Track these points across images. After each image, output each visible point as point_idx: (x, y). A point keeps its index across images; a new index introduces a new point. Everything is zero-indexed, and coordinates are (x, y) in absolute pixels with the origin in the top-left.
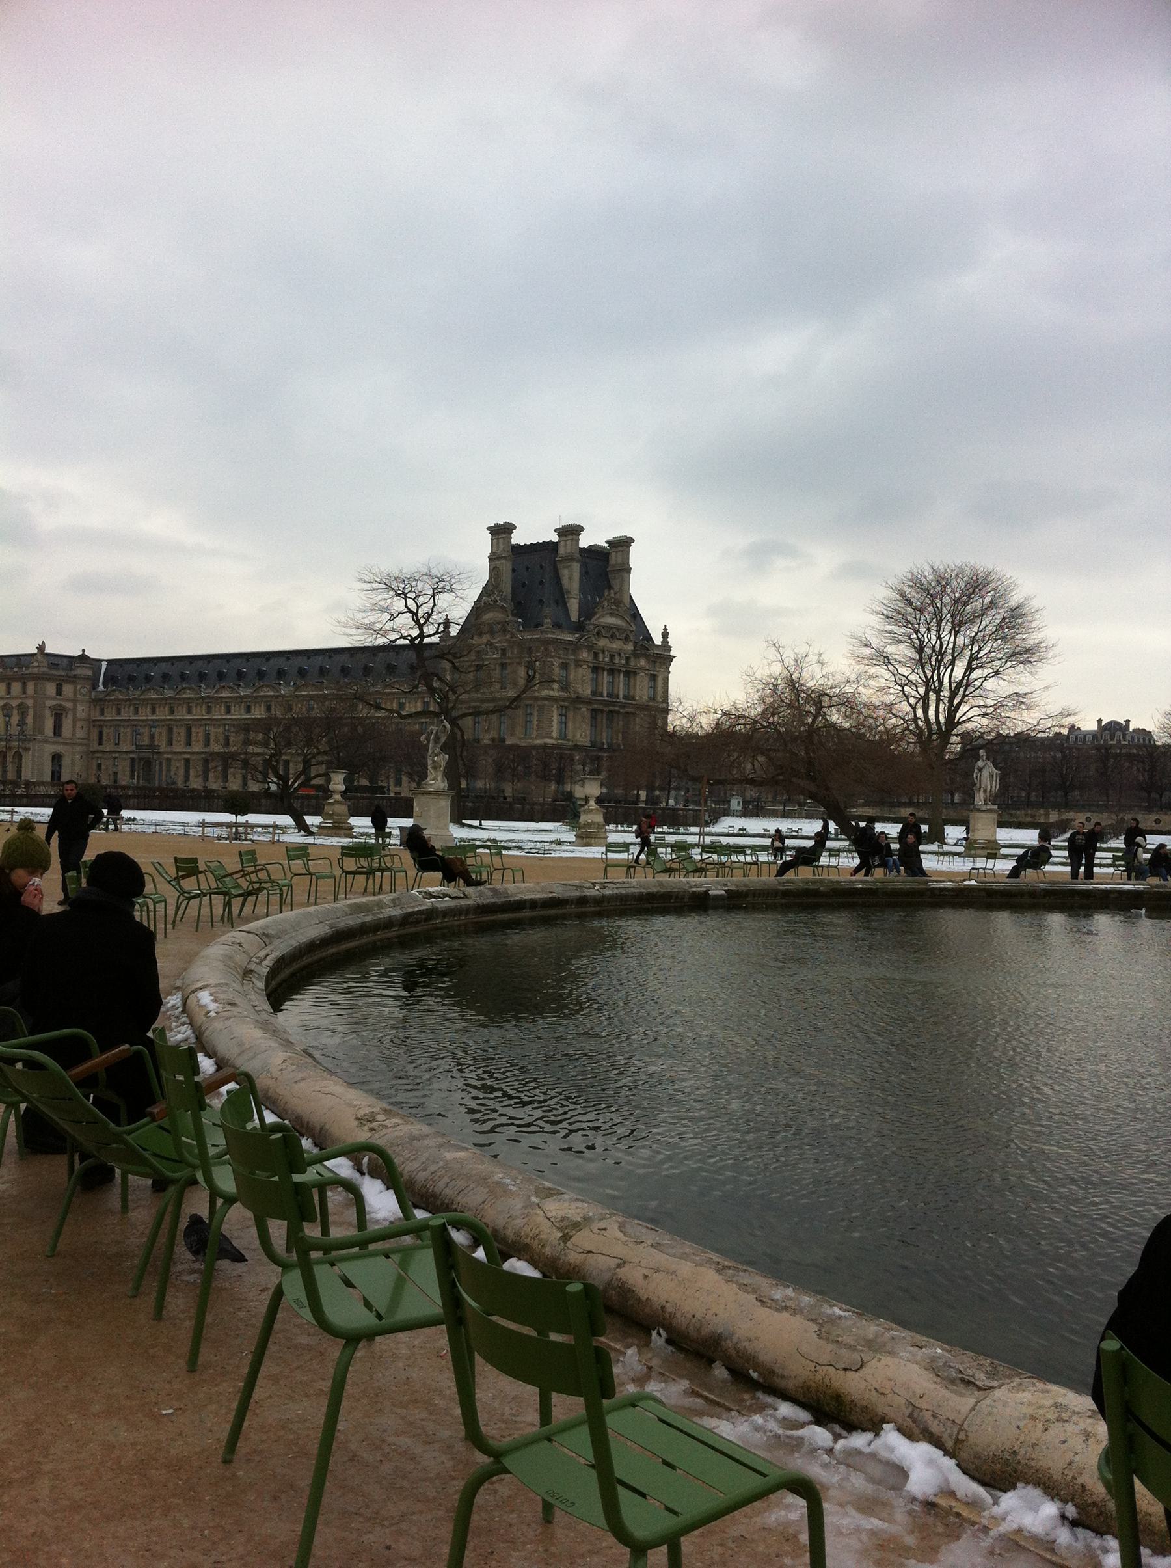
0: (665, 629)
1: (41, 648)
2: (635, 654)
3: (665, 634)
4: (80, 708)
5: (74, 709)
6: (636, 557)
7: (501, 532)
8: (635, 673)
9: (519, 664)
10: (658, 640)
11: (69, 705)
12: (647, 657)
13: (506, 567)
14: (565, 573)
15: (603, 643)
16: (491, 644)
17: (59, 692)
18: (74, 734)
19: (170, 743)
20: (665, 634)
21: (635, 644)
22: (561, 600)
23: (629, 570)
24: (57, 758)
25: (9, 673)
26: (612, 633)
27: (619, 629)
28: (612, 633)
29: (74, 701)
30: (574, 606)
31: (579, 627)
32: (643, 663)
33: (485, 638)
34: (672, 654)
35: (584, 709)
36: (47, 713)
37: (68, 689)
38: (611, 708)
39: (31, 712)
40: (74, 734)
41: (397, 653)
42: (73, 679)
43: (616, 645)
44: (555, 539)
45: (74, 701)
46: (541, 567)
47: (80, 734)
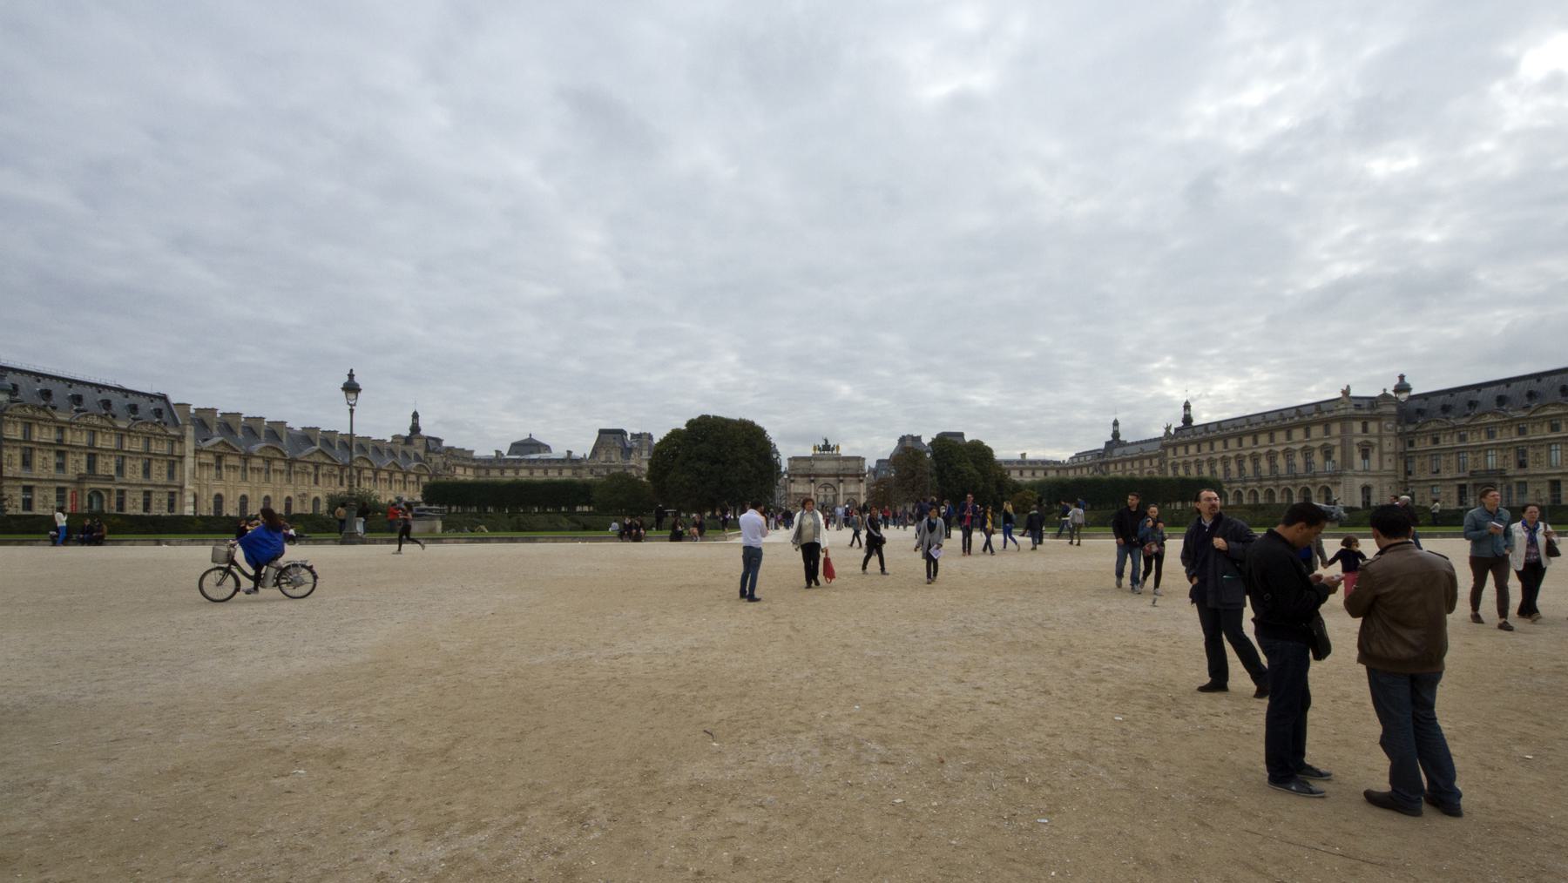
1: (1346, 392)
4: (1386, 442)
11: (1374, 440)
17: (1365, 430)
18: (1381, 466)
19: (1522, 465)
24: (1366, 490)
25: (1307, 419)
29: (1380, 437)
36: (1356, 449)
37: (1373, 427)
39: (1338, 451)
40: (1381, 466)
42: (1378, 418)
45: (1380, 437)
47: (1388, 466)
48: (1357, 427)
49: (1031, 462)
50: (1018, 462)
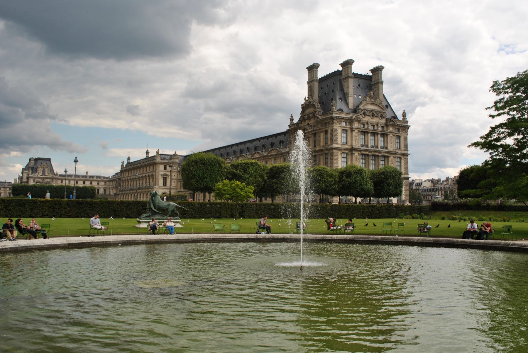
0: (404, 112)
2: (387, 125)
3: (404, 115)
4: (173, 174)
5: (171, 175)
6: (385, 75)
7: (313, 69)
8: (387, 135)
9: (322, 132)
10: (400, 118)
11: (169, 173)
12: (393, 126)
13: (316, 85)
14: (345, 84)
15: (366, 119)
16: (309, 124)
17: (165, 168)
20: (404, 115)
21: (387, 120)
22: (345, 98)
23: (382, 83)
26: (373, 114)
27: (376, 112)
28: (373, 114)
30: (351, 101)
31: (355, 111)
32: (391, 129)
33: (307, 122)
34: (408, 124)
35: (357, 154)
36: (160, 177)
38: (373, 153)
41: (276, 137)
43: (375, 120)
44: (340, 69)
46: (334, 83)
48: (161, 167)
49: (90, 177)
50: (83, 176)
